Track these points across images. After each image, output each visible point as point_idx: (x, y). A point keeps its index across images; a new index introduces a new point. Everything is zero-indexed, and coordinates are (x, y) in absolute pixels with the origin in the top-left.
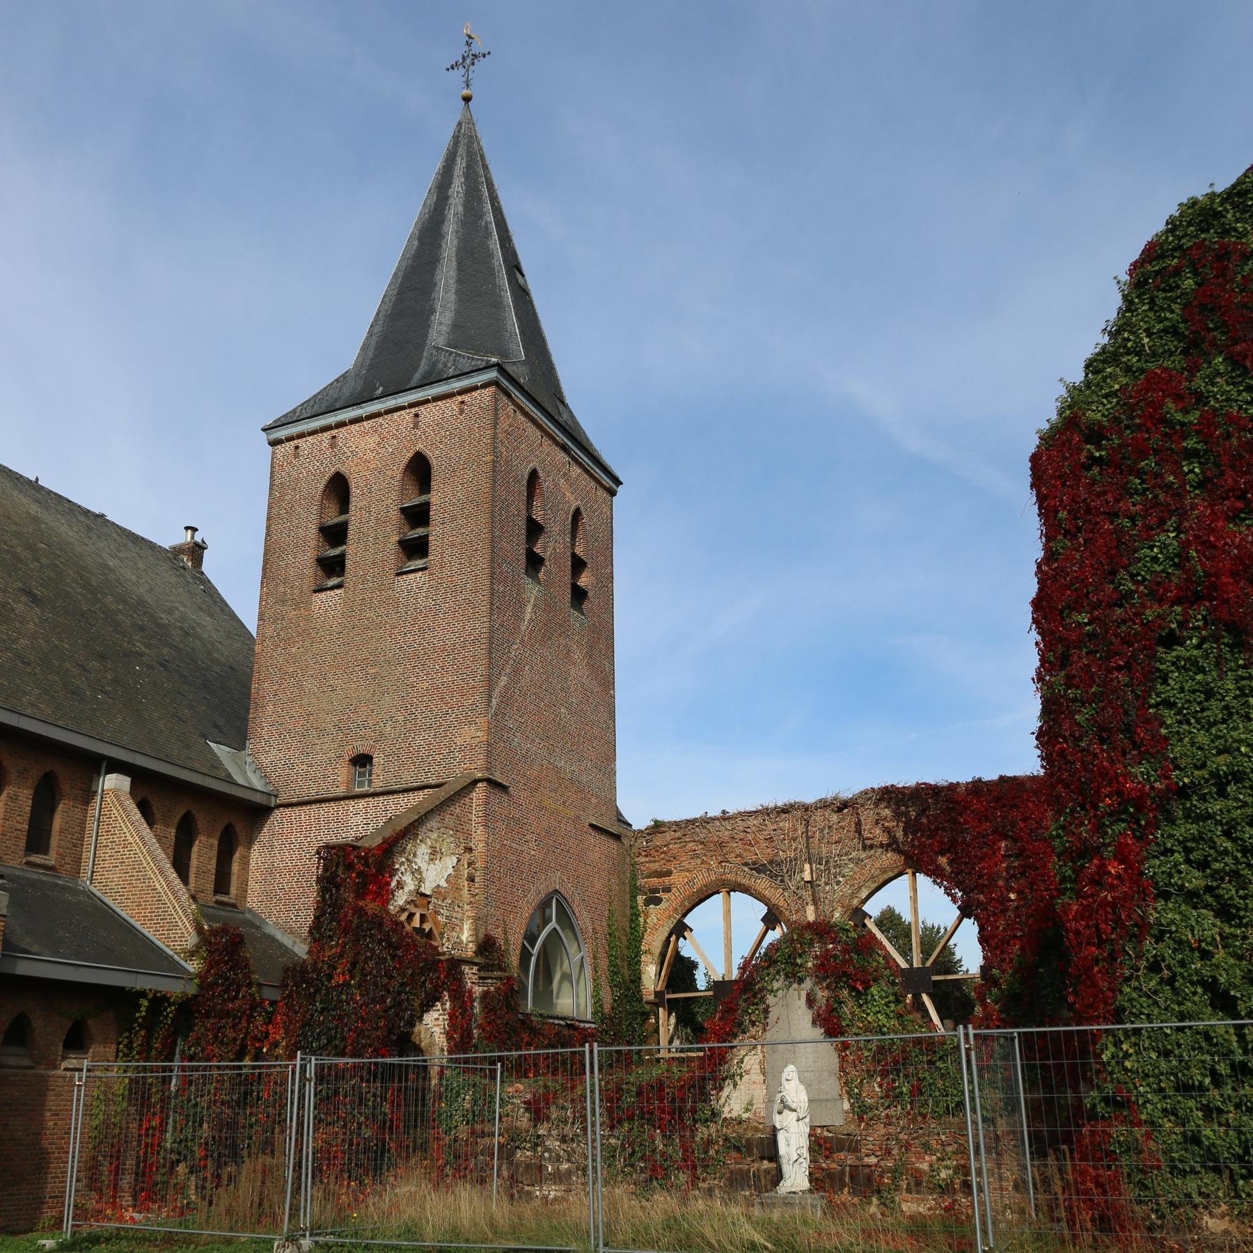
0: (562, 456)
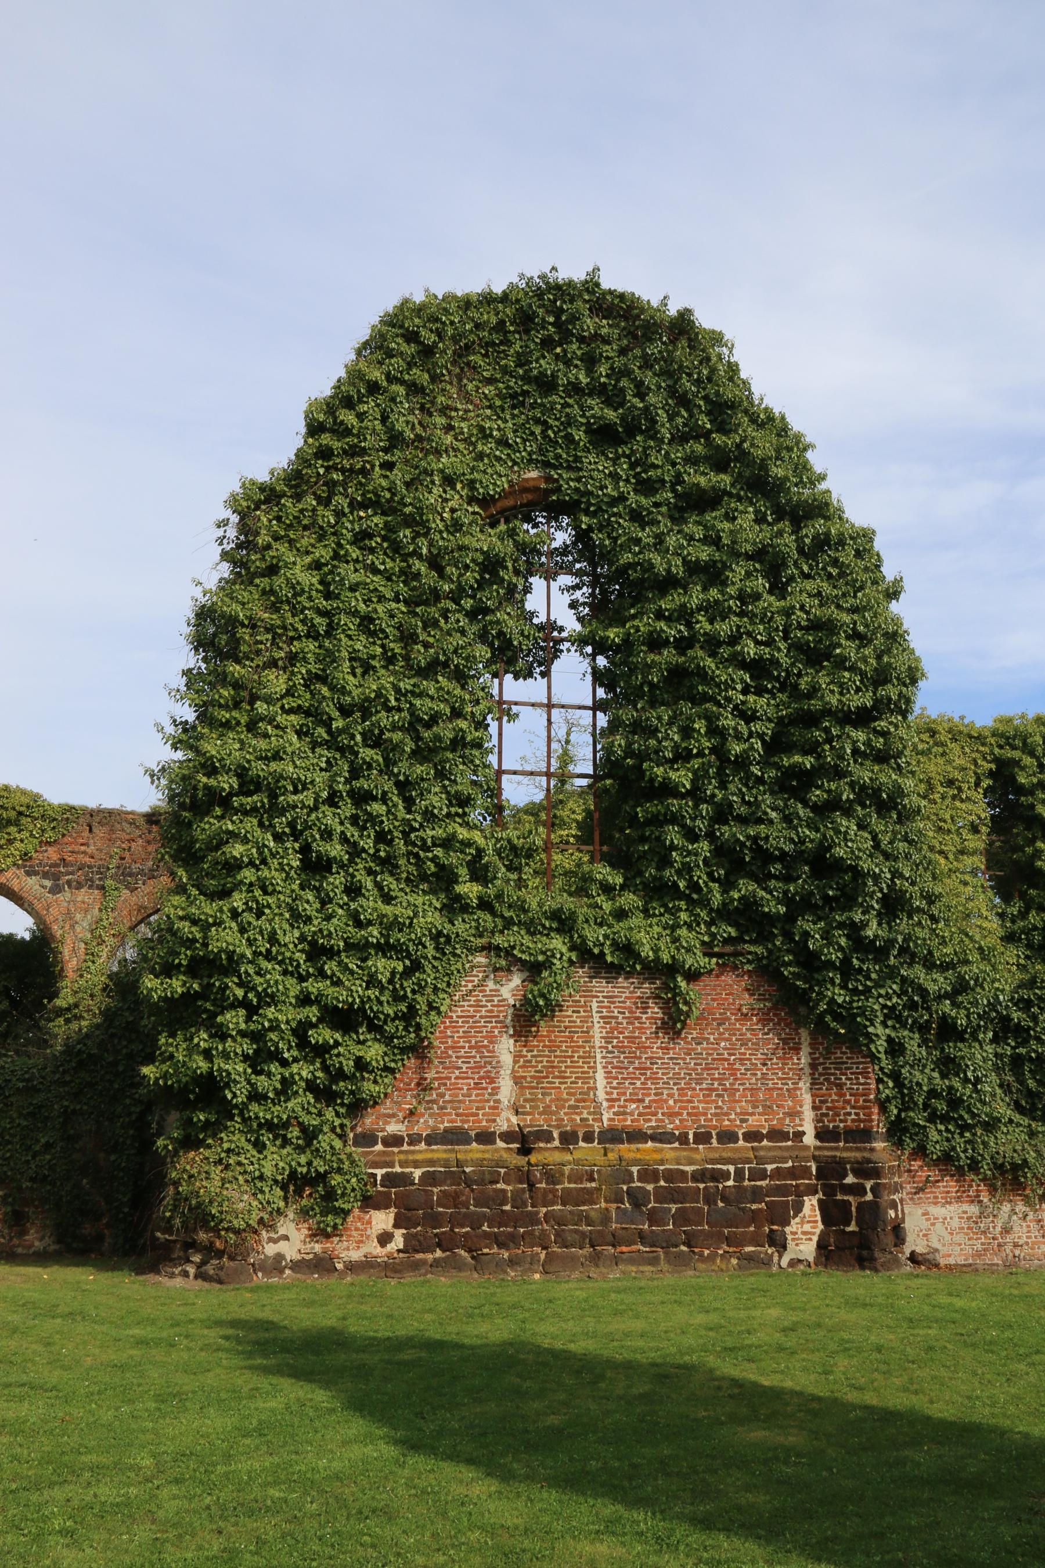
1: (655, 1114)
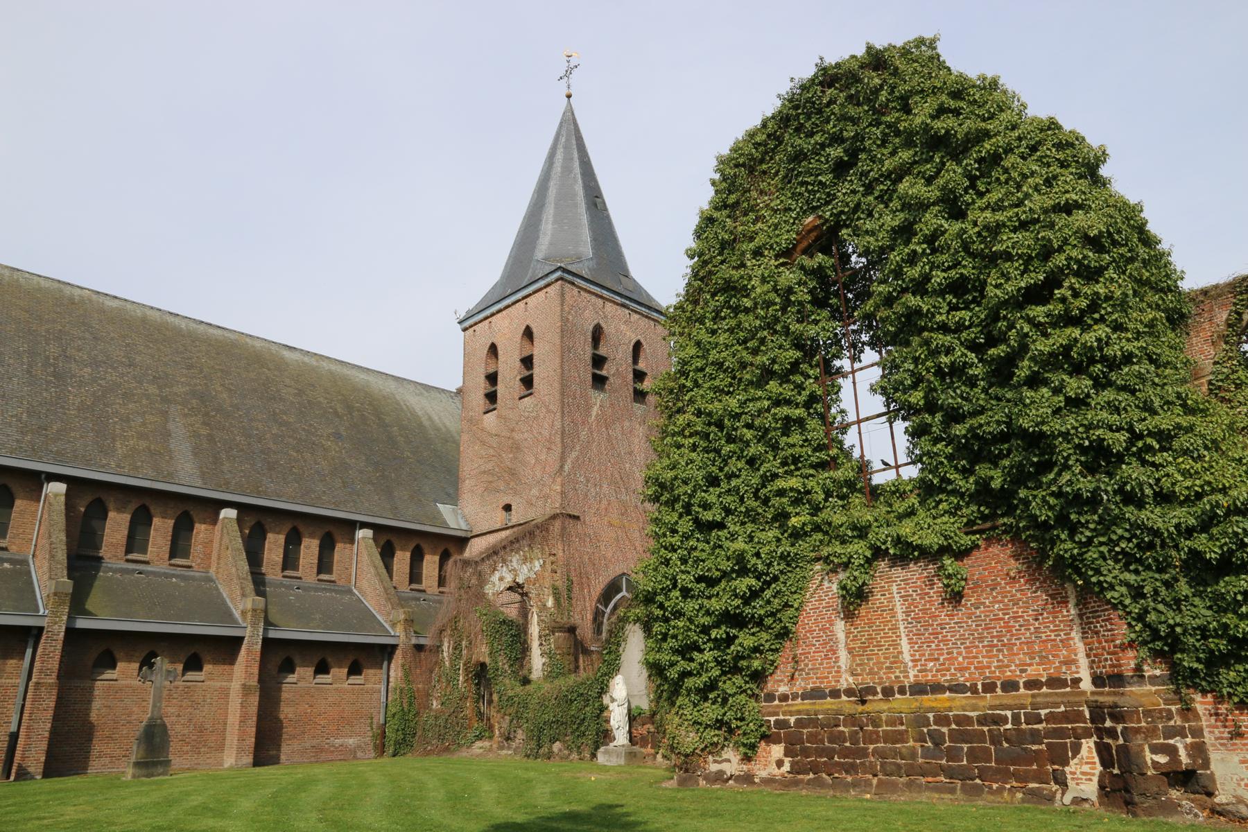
0: (621, 311)
1: (948, 670)
